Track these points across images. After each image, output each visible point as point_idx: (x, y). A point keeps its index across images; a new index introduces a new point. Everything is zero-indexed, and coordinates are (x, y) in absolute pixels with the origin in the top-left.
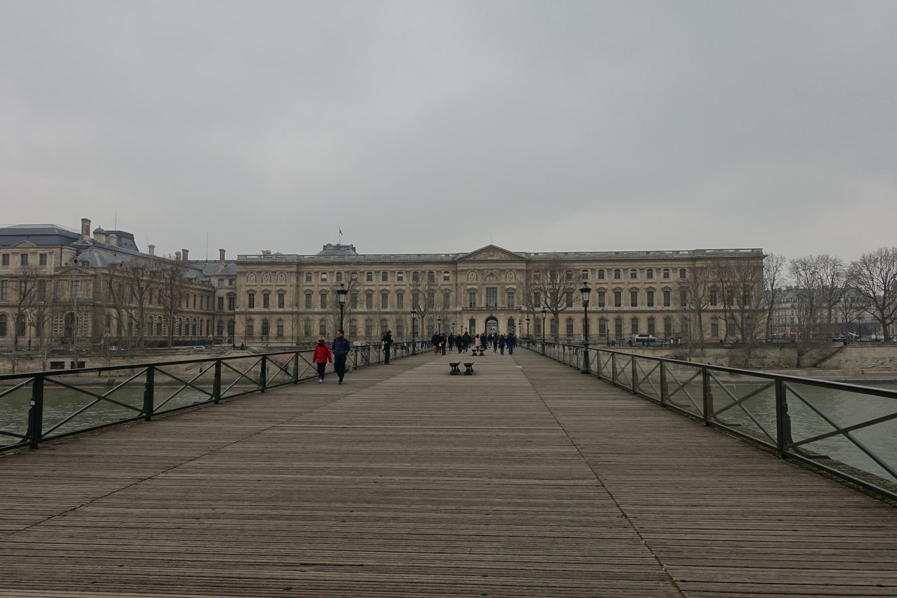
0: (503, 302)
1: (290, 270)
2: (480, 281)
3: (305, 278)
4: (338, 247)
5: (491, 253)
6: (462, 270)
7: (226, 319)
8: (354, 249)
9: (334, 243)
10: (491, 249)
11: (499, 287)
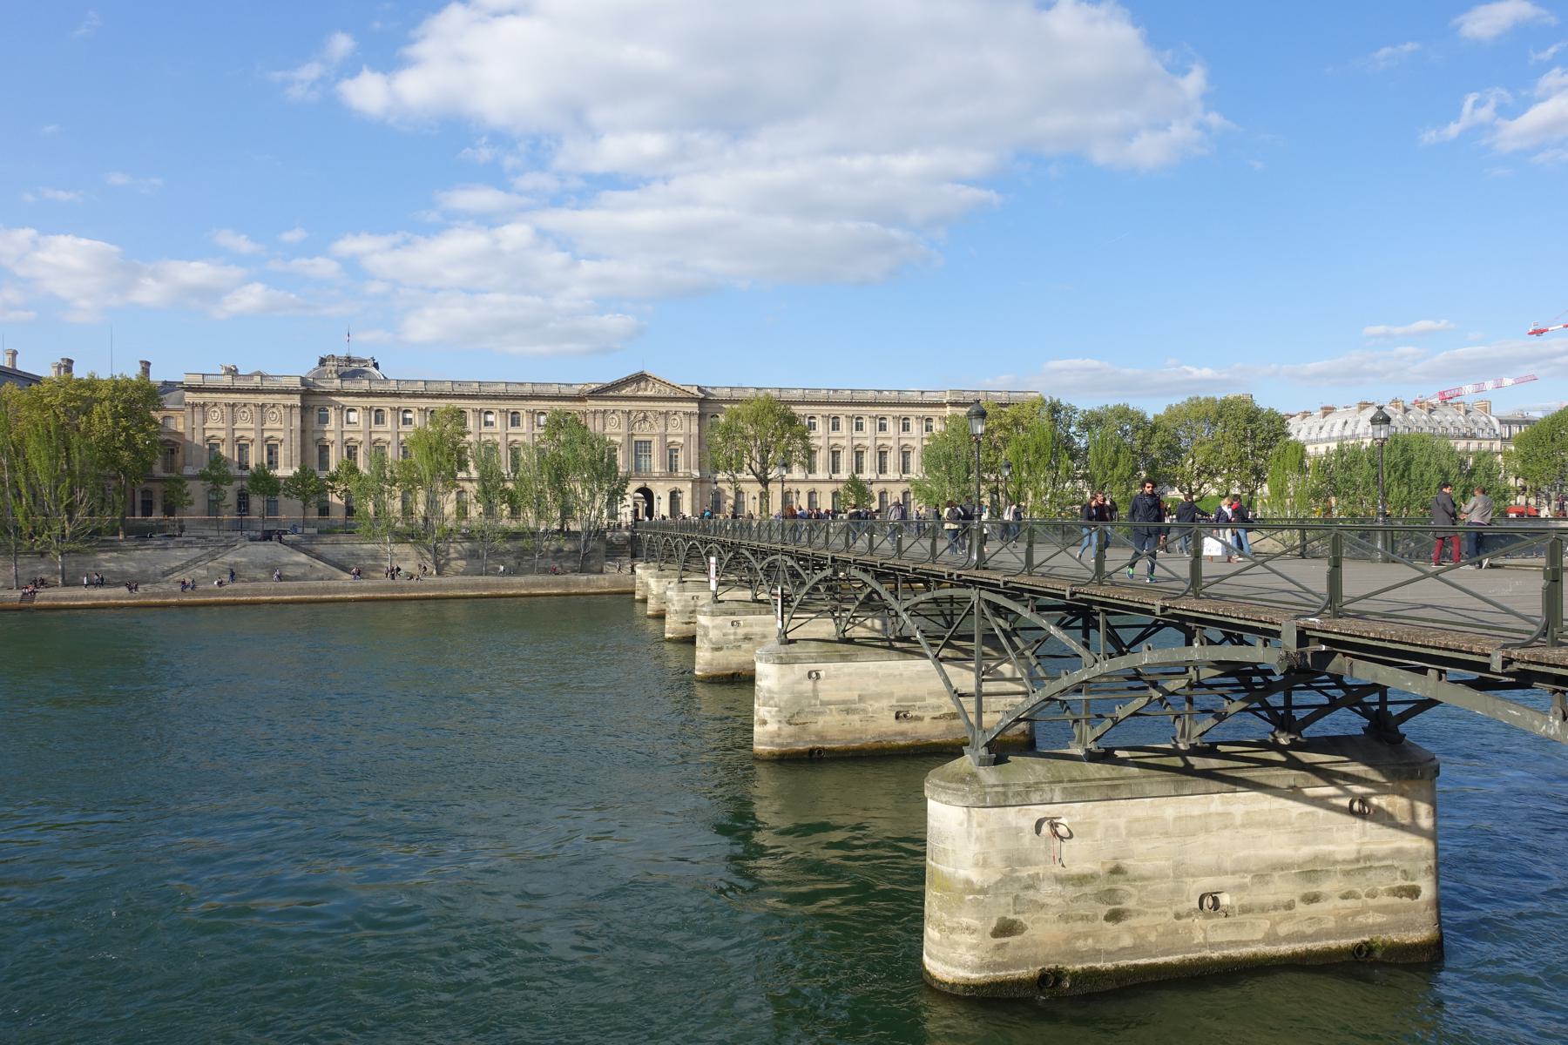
0: (662, 464)
1: (289, 403)
2: (623, 430)
3: (316, 418)
4: (349, 360)
5: (643, 385)
6: (595, 412)
7: (158, 489)
8: (376, 366)
9: (342, 354)
10: (641, 378)
11: (655, 440)
